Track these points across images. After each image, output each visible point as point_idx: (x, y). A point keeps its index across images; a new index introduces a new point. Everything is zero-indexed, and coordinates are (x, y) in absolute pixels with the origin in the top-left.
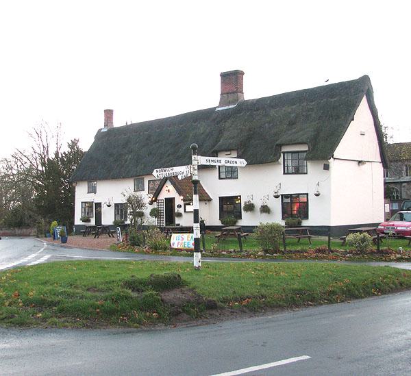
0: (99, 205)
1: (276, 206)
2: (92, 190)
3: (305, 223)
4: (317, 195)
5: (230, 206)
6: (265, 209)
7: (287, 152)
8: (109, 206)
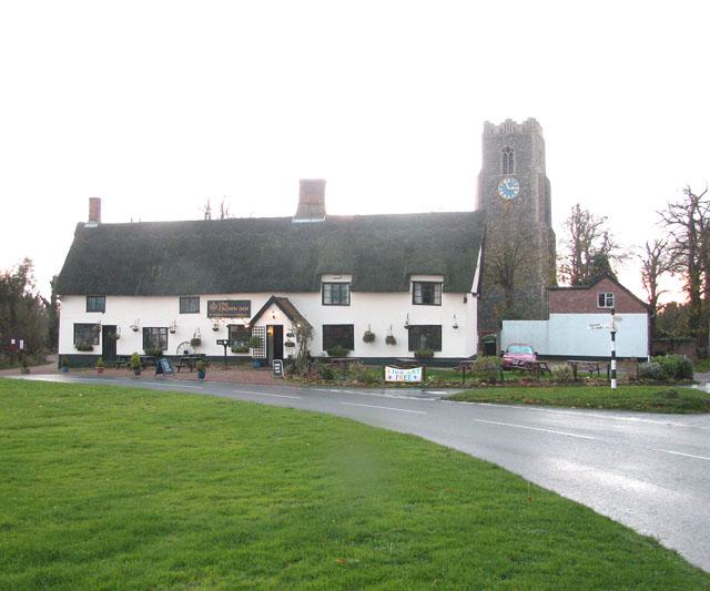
0: (112, 329)
1: (403, 337)
2: (96, 306)
3: (437, 355)
4: (456, 327)
5: (339, 337)
6: (391, 341)
7: (419, 282)
8: (136, 330)
